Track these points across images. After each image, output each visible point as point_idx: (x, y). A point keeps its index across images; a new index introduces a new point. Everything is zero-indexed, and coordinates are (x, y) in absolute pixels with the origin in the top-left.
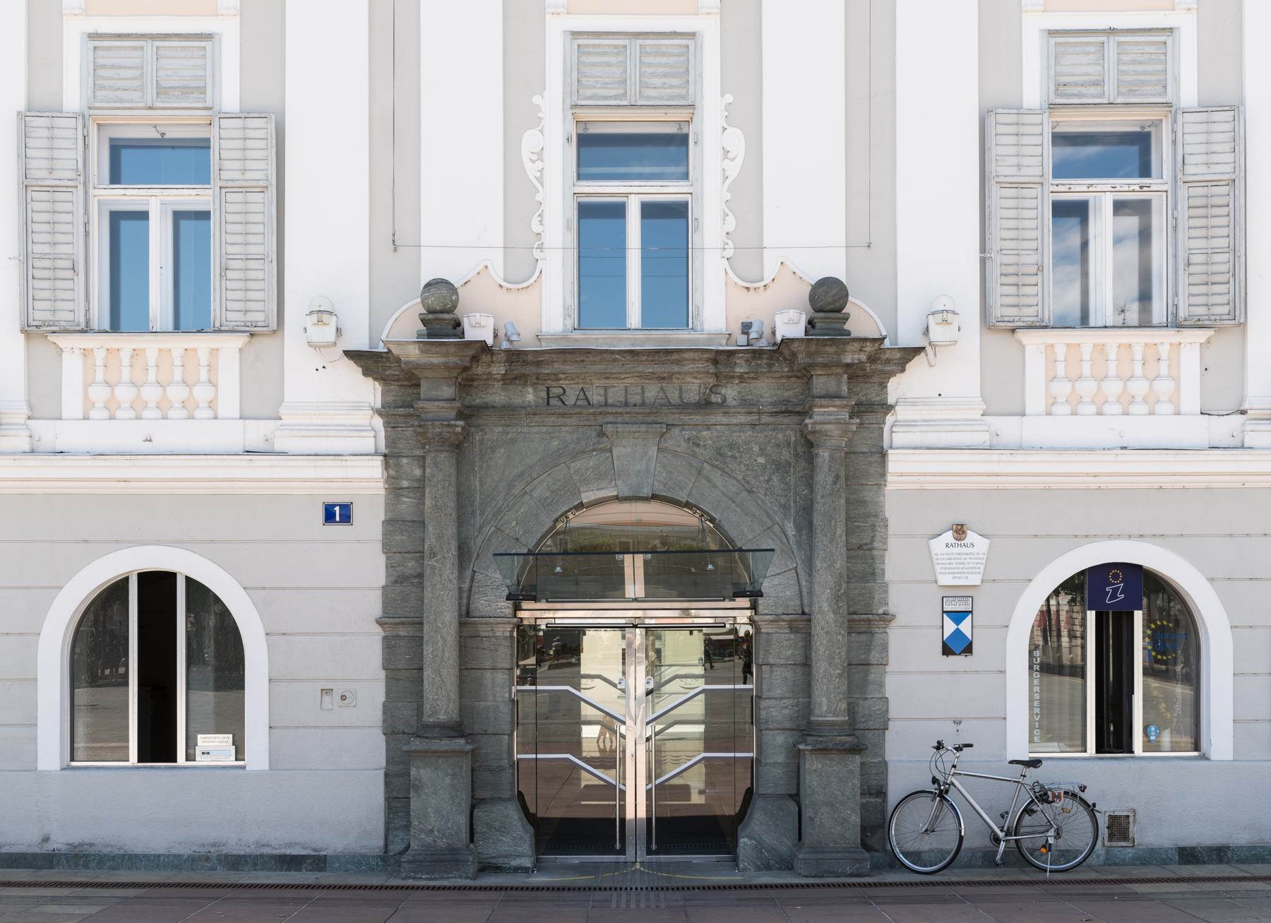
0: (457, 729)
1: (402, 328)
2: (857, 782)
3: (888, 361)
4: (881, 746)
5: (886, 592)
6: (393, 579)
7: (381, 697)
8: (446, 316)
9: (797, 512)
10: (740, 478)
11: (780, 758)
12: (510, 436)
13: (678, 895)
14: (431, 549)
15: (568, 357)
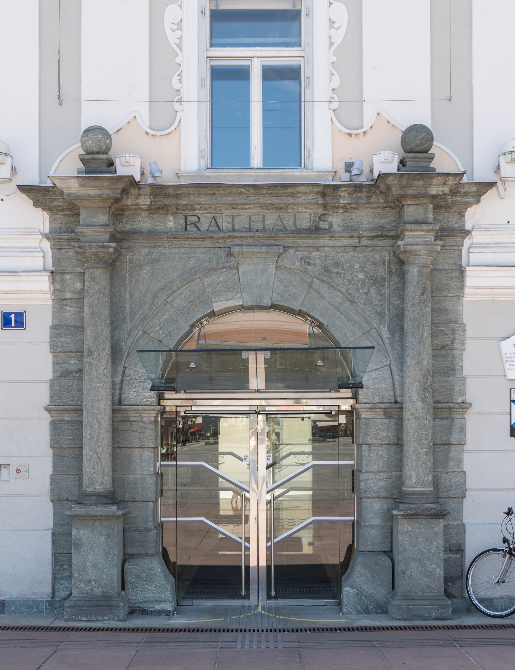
0: (111, 497)
1: (66, 166)
2: (441, 541)
3: (466, 194)
4: (460, 511)
5: (464, 384)
6: (58, 373)
7: (49, 471)
8: (101, 156)
9: (391, 319)
10: (343, 290)
11: (377, 521)
12: (154, 257)
13: (293, 636)
14: (89, 348)
15: (202, 190)
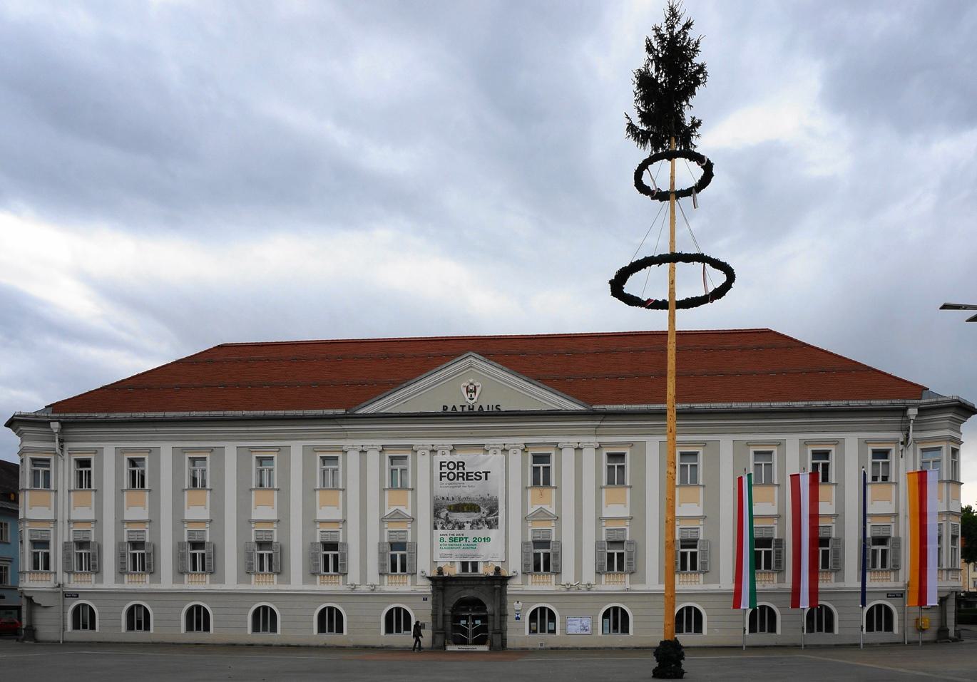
0: (442, 629)
